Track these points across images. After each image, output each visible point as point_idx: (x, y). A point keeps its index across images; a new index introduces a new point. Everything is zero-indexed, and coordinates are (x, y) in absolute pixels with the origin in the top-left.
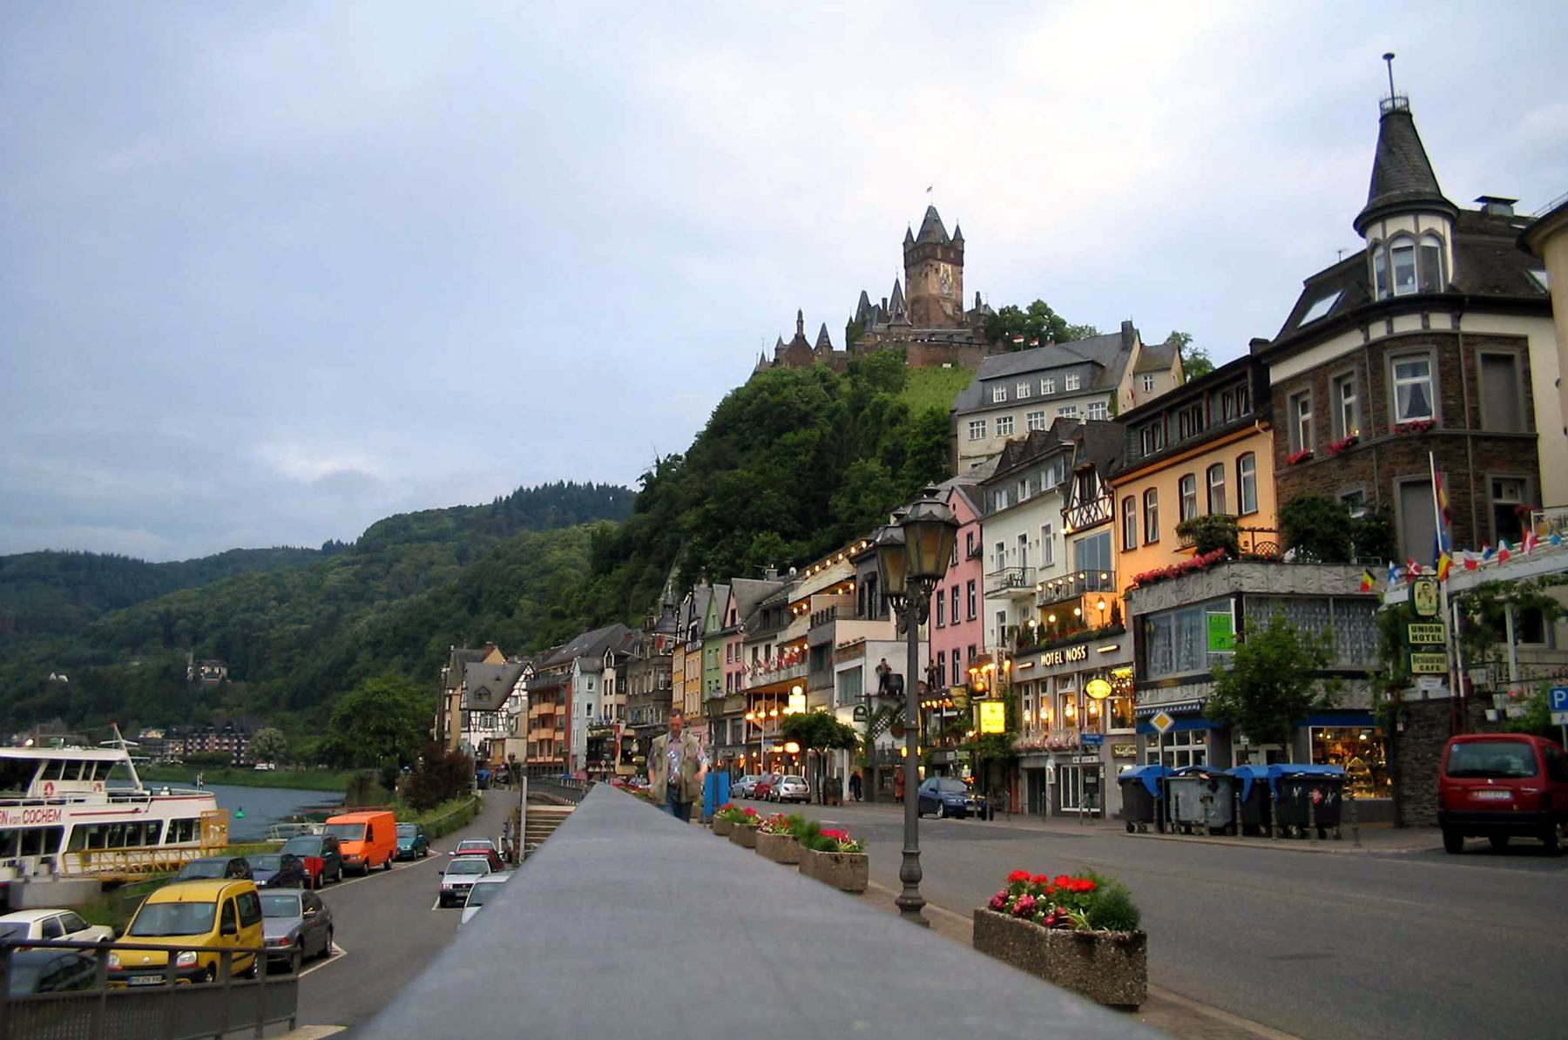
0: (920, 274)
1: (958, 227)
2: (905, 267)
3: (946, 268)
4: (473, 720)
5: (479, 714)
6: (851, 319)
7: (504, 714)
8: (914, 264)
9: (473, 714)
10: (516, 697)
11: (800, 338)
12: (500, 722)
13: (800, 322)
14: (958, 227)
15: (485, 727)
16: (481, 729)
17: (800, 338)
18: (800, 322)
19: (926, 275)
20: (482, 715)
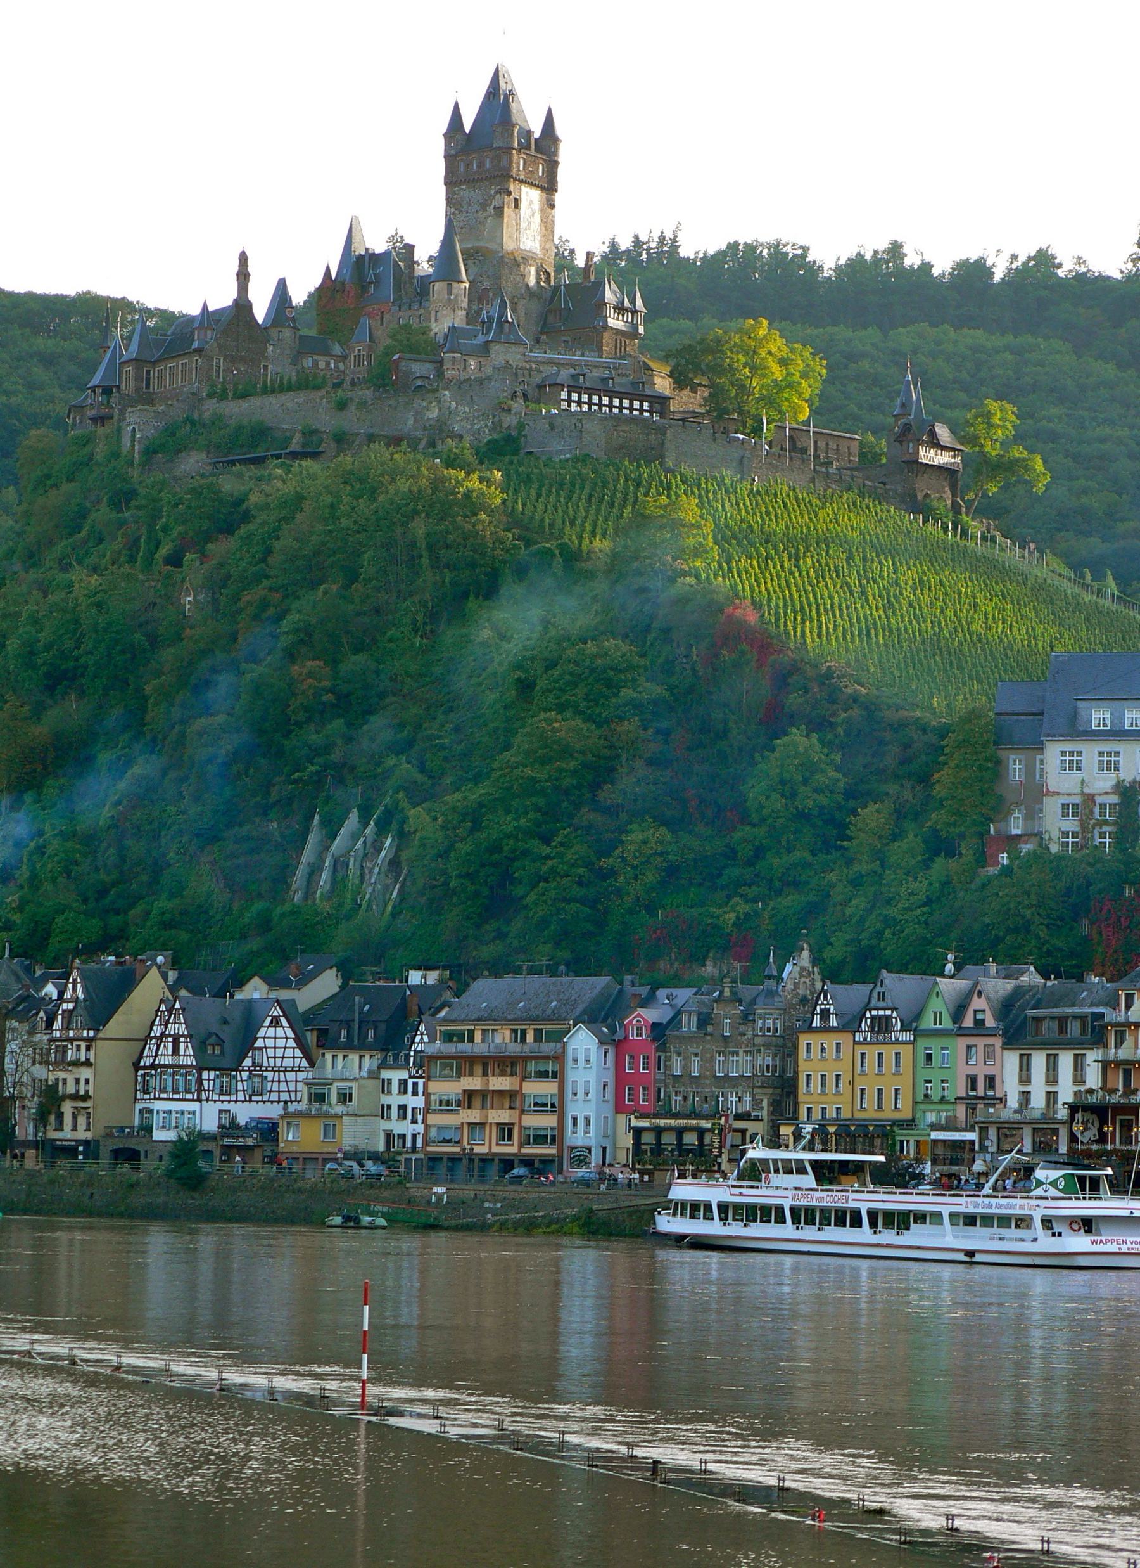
0: (484, 206)
1: (550, 114)
2: (452, 181)
3: (531, 197)
4: (205, 1083)
5: (212, 1074)
6: (328, 269)
7: (245, 1075)
8: (471, 181)
9: (205, 1075)
10: (260, 1049)
11: (242, 305)
12: (240, 1087)
13: (243, 276)
14: (550, 114)
15: (221, 1094)
16: (216, 1097)
17: (242, 305)
18: (243, 276)
20: (217, 1076)
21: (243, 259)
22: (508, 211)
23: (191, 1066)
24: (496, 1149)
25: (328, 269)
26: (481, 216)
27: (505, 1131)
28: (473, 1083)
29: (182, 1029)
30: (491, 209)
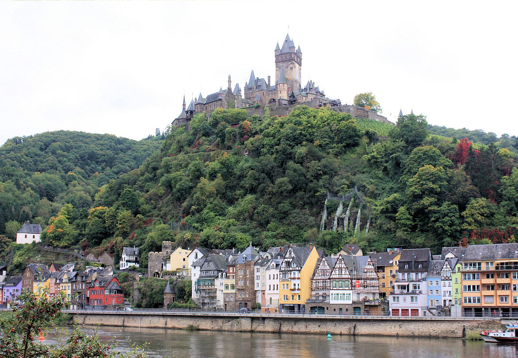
0: (287, 67)
3: (297, 65)
6: (246, 83)
11: (230, 89)
13: (230, 82)
17: (230, 89)
18: (230, 82)
19: (292, 68)
21: (229, 78)
22: (294, 68)
23: (348, 278)
24: (499, 305)
25: (246, 83)
26: (286, 70)
27: (503, 298)
28: (491, 281)
29: (343, 266)
30: (289, 68)
